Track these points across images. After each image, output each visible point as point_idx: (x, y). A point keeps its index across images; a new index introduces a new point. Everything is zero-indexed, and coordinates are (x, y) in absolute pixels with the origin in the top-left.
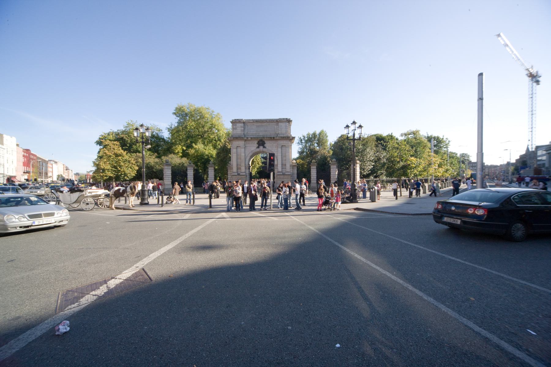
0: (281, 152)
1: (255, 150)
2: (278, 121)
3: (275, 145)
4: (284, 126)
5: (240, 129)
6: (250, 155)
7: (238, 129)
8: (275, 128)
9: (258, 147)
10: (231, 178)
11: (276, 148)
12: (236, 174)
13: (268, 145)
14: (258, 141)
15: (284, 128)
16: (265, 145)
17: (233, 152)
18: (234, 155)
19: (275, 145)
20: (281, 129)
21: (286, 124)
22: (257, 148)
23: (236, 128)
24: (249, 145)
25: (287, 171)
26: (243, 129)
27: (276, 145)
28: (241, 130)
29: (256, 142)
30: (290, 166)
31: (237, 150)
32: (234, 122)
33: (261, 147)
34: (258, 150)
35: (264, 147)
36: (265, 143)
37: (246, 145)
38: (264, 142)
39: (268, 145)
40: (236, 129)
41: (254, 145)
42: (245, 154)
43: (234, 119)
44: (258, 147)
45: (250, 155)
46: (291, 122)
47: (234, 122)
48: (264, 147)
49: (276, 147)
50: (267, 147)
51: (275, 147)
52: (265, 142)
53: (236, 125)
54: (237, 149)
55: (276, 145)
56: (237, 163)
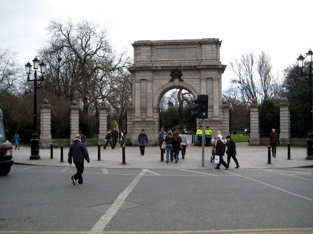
0: (206, 86)
1: (167, 84)
2: (201, 43)
3: (196, 77)
4: (210, 49)
5: (146, 54)
6: (160, 91)
7: (142, 54)
8: (196, 52)
9: (172, 80)
10: (132, 126)
11: (197, 81)
12: (140, 120)
13: (188, 77)
14: (172, 72)
15: (211, 52)
16: (182, 77)
17: (135, 88)
18: (136, 91)
19: (196, 77)
20: (206, 54)
21: (213, 47)
22: (170, 81)
23: (140, 53)
24: (159, 78)
25: (214, 115)
26: (150, 54)
27: (199, 77)
28: (147, 56)
29: (169, 73)
30: (219, 108)
31: (140, 85)
32: (137, 45)
33: (177, 81)
34: (172, 84)
35: (181, 80)
36: (182, 75)
37: (154, 78)
38: (180, 72)
39: (188, 77)
40: (140, 54)
41: (166, 77)
42: (153, 91)
43: (137, 40)
44: (172, 80)
45: (160, 91)
46: (221, 43)
47: (137, 45)
48: (181, 80)
49: (199, 80)
50: (185, 80)
51: (196, 80)
52: (183, 73)
53: (140, 50)
54: (140, 82)
55: (199, 77)
56: (141, 105)
